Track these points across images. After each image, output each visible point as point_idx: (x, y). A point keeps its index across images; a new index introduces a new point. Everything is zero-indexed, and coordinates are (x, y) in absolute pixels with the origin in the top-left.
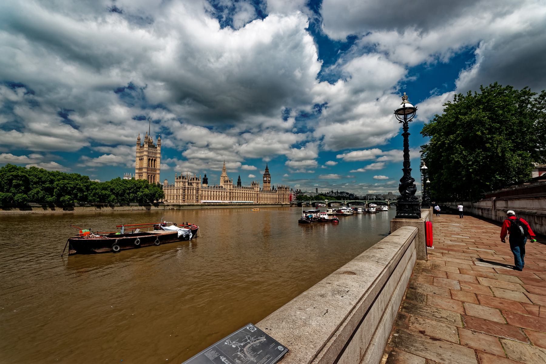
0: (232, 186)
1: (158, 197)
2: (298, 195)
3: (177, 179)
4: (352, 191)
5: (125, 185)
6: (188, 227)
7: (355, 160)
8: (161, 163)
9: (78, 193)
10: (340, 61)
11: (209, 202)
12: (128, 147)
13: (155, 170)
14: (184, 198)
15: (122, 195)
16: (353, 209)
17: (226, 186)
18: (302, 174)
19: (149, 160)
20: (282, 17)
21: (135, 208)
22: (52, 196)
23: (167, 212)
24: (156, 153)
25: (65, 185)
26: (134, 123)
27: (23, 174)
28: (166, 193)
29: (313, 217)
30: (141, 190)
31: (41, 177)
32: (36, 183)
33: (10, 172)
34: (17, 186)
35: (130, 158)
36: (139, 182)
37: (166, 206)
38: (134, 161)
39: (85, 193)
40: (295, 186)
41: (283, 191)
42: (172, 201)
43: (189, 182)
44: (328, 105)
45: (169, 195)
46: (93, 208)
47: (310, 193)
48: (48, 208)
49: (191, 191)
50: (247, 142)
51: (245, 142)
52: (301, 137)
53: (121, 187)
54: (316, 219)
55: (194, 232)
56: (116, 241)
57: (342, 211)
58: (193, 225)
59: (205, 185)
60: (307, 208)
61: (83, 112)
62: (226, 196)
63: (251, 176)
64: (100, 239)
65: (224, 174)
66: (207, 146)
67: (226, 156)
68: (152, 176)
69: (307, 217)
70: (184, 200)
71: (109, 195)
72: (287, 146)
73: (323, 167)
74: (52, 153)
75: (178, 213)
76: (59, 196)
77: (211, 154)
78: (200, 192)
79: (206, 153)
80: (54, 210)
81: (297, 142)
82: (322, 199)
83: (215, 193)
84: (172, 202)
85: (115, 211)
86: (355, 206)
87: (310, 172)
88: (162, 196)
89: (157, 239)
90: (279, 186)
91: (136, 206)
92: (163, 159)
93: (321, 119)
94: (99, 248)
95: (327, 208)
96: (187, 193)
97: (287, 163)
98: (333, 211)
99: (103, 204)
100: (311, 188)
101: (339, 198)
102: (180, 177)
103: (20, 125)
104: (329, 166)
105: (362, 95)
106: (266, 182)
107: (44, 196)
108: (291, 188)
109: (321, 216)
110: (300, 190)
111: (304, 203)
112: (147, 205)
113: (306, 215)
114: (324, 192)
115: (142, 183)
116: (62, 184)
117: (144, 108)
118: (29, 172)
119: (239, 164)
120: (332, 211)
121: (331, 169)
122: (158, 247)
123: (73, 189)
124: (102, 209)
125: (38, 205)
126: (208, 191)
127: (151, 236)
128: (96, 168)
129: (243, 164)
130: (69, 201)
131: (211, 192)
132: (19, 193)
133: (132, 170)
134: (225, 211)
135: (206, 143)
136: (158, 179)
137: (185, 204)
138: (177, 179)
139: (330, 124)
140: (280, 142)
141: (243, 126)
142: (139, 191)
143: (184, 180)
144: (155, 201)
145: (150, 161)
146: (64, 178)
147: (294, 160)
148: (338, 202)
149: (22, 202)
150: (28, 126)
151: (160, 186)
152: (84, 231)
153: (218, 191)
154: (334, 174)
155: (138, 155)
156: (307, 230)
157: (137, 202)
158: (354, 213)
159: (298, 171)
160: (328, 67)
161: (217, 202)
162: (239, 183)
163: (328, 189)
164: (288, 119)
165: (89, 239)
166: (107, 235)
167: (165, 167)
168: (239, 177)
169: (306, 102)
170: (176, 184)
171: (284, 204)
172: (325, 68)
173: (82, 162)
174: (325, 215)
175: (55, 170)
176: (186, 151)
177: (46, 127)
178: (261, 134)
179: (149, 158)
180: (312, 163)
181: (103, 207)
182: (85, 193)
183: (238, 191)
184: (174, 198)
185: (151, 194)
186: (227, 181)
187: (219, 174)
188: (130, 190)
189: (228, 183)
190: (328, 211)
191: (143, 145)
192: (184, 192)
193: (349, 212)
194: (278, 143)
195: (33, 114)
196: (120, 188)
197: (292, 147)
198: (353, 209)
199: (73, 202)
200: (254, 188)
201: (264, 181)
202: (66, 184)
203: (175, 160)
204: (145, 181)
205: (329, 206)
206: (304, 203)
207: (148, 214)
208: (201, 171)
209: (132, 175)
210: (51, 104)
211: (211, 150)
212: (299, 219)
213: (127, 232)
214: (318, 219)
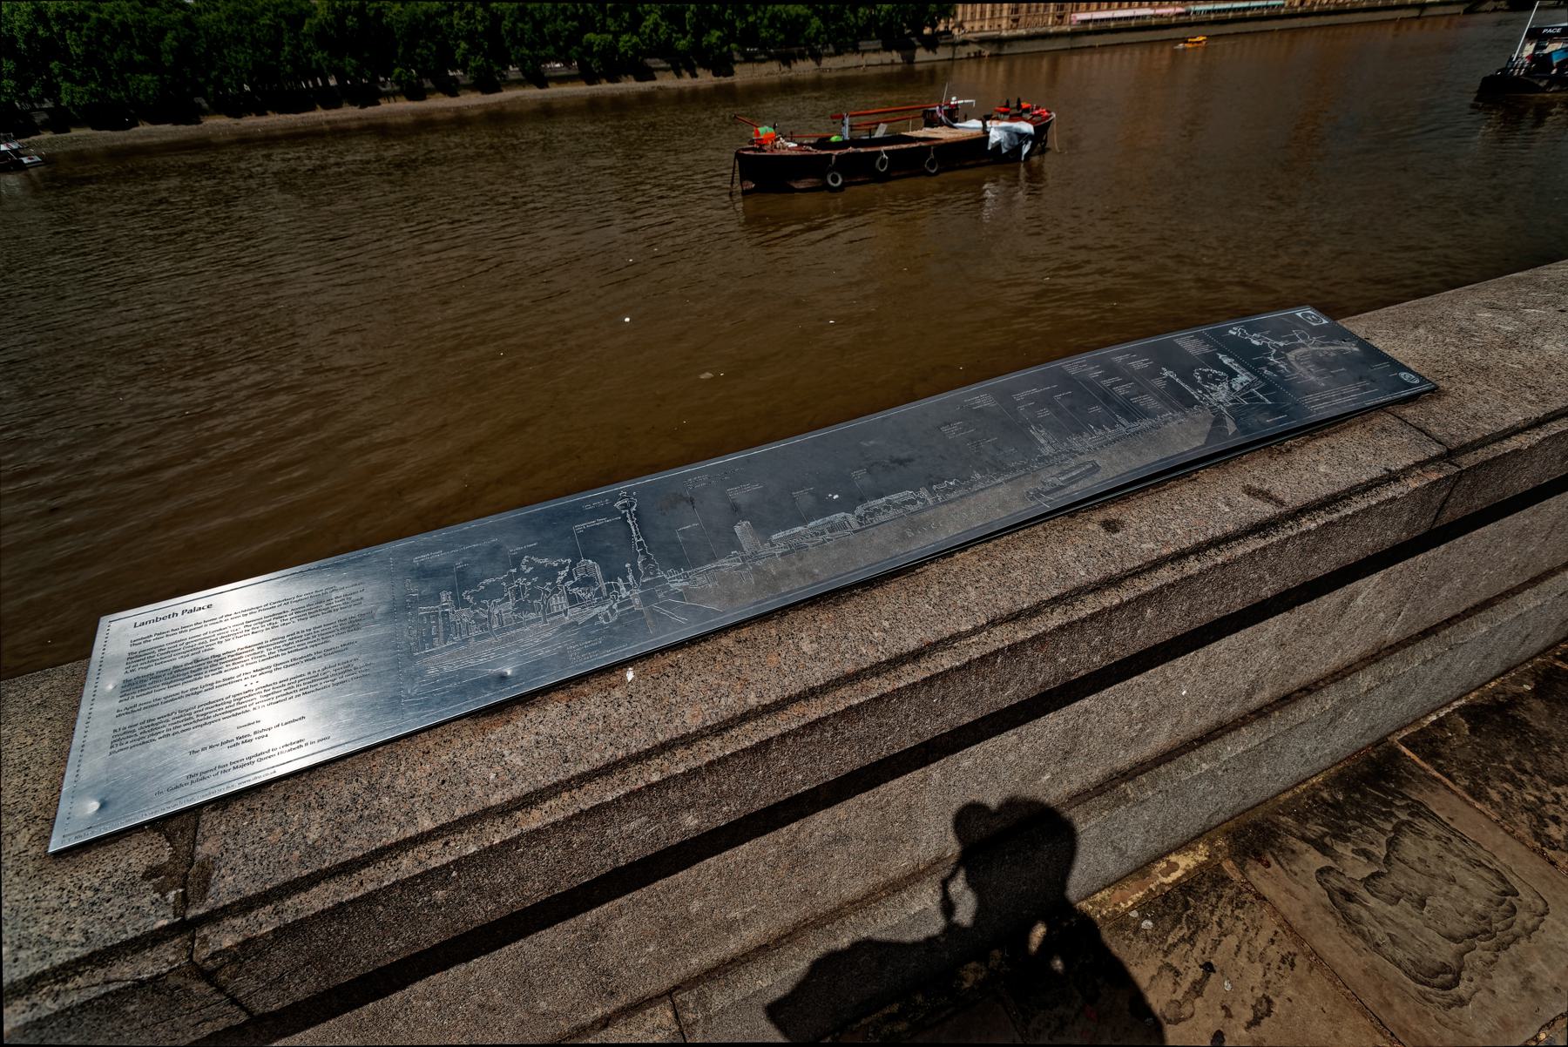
11: (1102, 20)
21: (874, 58)
22: (685, 34)
37: (957, 44)
39: (751, 19)
42: (977, 25)
46: (774, 66)
48: (683, 71)
56: (834, 158)
58: (1038, 108)
64: (799, 153)
71: (807, 19)
75: (993, 65)
80: (696, 76)
84: (976, 29)
85: (824, 70)
91: (875, 51)
94: (798, 179)
99: (795, 50)
107: (670, 36)
112: (906, 48)
113: (1536, 48)
124: (794, 66)
125: (663, 65)
127: (914, 145)
130: (720, 48)
144: (927, 31)
152: (762, 130)
157: (878, 38)
161: (1132, 18)
165: (777, 153)
166: (812, 142)
181: (796, 62)
182: (751, 19)
199: (730, 50)
207: (908, 77)
212: (1492, 69)
213: (857, 134)
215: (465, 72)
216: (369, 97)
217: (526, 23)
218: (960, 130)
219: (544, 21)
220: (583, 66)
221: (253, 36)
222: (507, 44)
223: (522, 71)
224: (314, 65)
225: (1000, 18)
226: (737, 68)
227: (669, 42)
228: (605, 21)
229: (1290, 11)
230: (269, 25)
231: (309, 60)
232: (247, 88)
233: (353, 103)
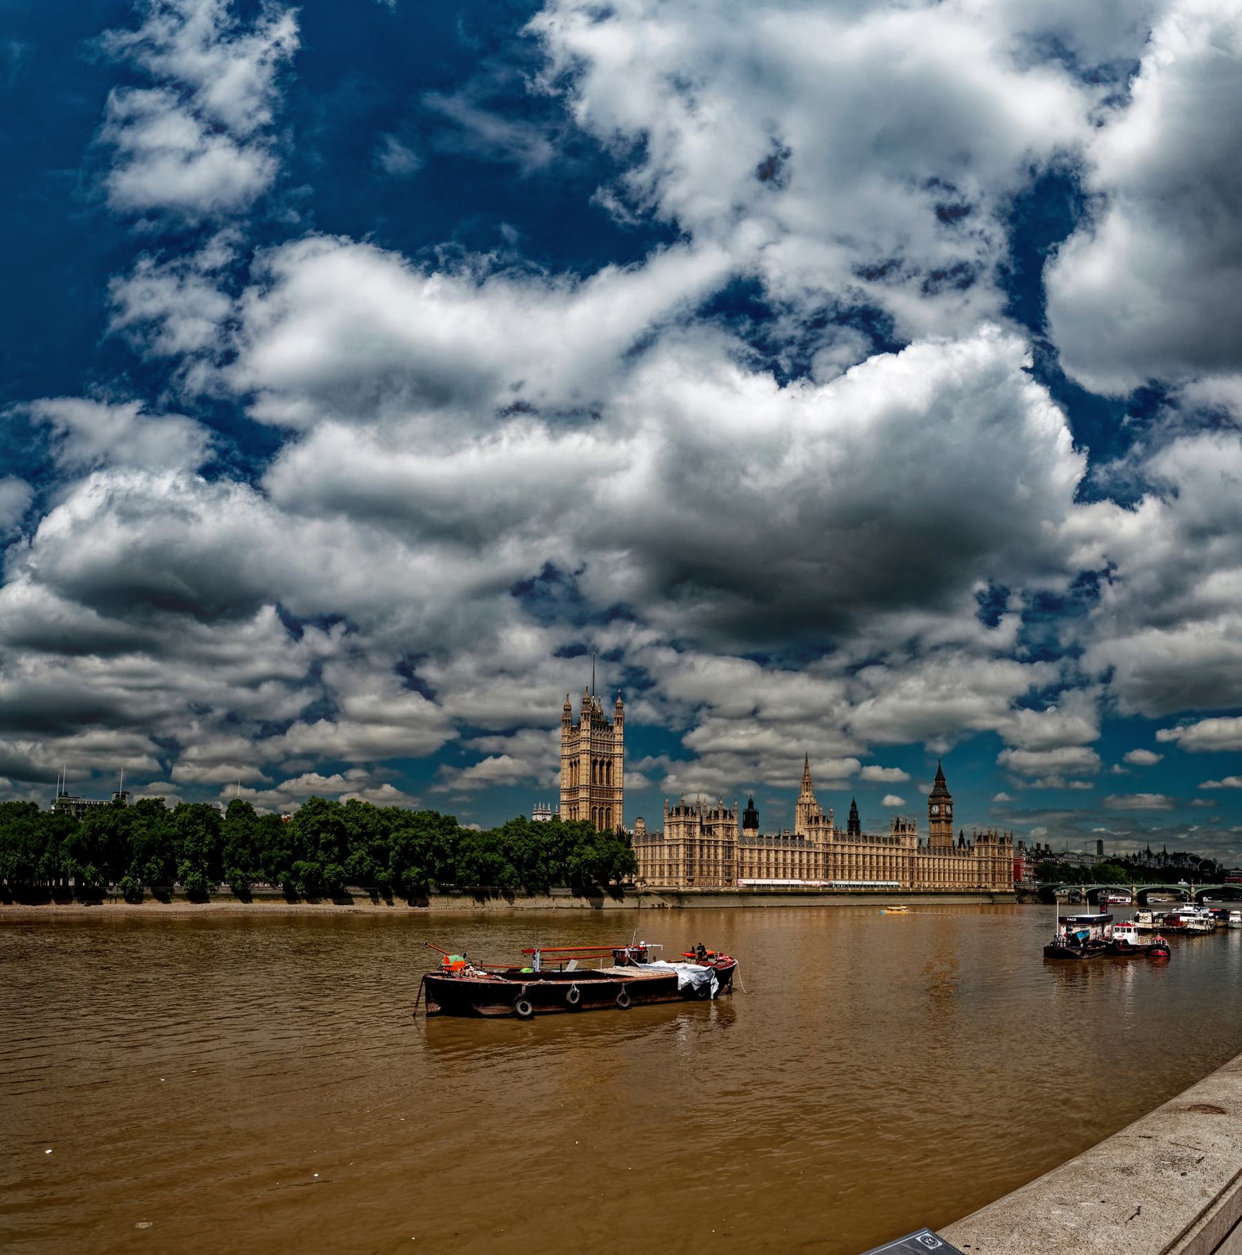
0: (831, 835)
1: (619, 870)
2: (1042, 861)
3: (670, 815)
4: (1208, 851)
5: (537, 837)
6: (706, 960)
7: (1214, 747)
8: (625, 770)
9: (434, 861)
10: (1137, 448)
11: (764, 885)
12: (542, 732)
13: (610, 791)
14: (691, 873)
15: (531, 864)
16: (1216, 913)
17: (813, 834)
18: (1050, 792)
19: (594, 763)
20: (943, 344)
22: (387, 868)
23: (647, 916)
24: (611, 745)
25: (408, 839)
26: (557, 667)
27: (337, 818)
28: (642, 858)
29: (1092, 937)
30: (575, 849)
31: (367, 824)
32: (358, 838)
33: (316, 814)
34: (327, 846)
35: (547, 761)
36: (571, 828)
37: (641, 895)
38: (557, 770)
39: (450, 861)
40: (1032, 832)
41: (994, 847)
42: (657, 882)
43: (704, 823)
44: (1119, 572)
45: (649, 863)
47: (1078, 856)
48: (381, 899)
49: (709, 851)
50: (874, 693)
51: (869, 693)
52: (1046, 673)
53: (527, 842)
54: (1101, 943)
55: (725, 976)
57: (1183, 919)
58: (721, 955)
59: (749, 833)
60: (1071, 908)
61: (444, 654)
62: (813, 867)
63: (891, 800)
65: (807, 797)
66: (754, 715)
67: (809, 740)
68: (602, 808)
69: (1073, 939)
70: (692, 877)
71: (502, 866)
72: (1002, 702)
73: (1117, 768)
74: (384, 764)
75: (676, 918)
76: (400, 867)
77: (767, 738)
78: (736, 852)
79: (752, 735)
81: (1032, 688)
82: (1113, 878)
83: (781, 855)
84: (657, 884)
85: (516, 908)
86: (1220, 904)
87: (1078, 785)
88: (630, 866)
89: (623, 991)
90: (978, 834)
91: (565, 897)
92: (632, 756)
93: (1098, 618)
94: (487, 1004)
95: (1134, 908)
96: (698, 857)
97: (1004, 756)
98: (1153, 918)
99: (489, 888)
100: (1083, 840)
101: (1170, 875)
102: (678, 810)
103: (331, 706)
104: (1138, 768)
105: (1217, 545)
106: (939, 821)
107: (373, 868)
108: (1017, 837)
109: (1116, 936)
110: (1047, 846)
111: (1063, 891)
113: (1067, 930)
114: (1122, 853)
115: (578, 831)
116: (404, 838)
117: (579, 622)
118: (346, 812)
119: (852, 764)
120: (1149, 920)
121: (1141, 779)
122: (626, 1014)
123: (426, 848)
124: (487, 903)
125: (363, 893)
126: (760, 850)
127: (605, 981)
128: (471, 793)
129: (865, 762)
130: (418, 882)
131: (768, 855)
132: (331, 863)
133: (552, 795)
134: (815, 913)
135: (749, 704)
136: (617, 817)
137: (694, 889)
138: (670, 815)
139: (1129, 634)
140: (978, 689)
141: (861, 647)
142: (569, 854)
143: (690, 819)
144: (612, 882)
145: (598, 767)
146: (407, 825)
147: (1026, 746)
148: (1170, 891)
149: (336, 884)
150: (344, 707)
151: (625, 839)
153: (789, 848)
154: (1155, 793)
155: (567, 752)
156: (1071, 976)
158: (1216, 927)
159: (1039, 784)
160: (1104, 462)
161: (788, 885)
162: (854, 825)
163: (1135, 844)
164: (1000, 617)
165: (465, 980)
167: (636, 781)
168: (854, 805)
169: (1050, 565)
170: (667, 829)
171: (997, 890)
172: (1097, 466)
173: (441, 780)
174: (1129, 931)
175: (390, 805)
176: (693, 730)
177: (373, 703)
178: (917, 667)
179: (593, 758)
180: (1083, 756)
182: (450, 861)
183: (852, 850)
184: (662, 873)
185: (601, 860)
186: (817, 819)
187: (791, 796)
188: (548, 850)
189: (821, 826)
190: (1137, 919)
191: (579, 724)
192: (691, 855)
193: (1201, 922)
194: (970, 693)
195: (353, 677)
196: (526, 845)
197: (1016, 705)
198: (1216, 913)
199: (426, 883)
200: (902, 840)
201: (931, 816)
202: (411, 839)
203: (664, 759)
204: (585, 823)
205: (1141, 902)
206: (1063, 891)
207: (599, 920)
208: (737, 788)
209: (553, 807)
210: (382, 647)
211: (765, 723)
212: (1048, 944)
214: (1106, 944)
215: (182, 884)
216: (95, 896)
217: (245, 849)
218: (651, 970)
219: (262, 848)
220: (288, 887)
221: (25, 844)
222: (225, 865)
223: (233, 888)
224: (62, 870)
225: (677, 877)
226: (432, 901)
227: (371, 873)
228: (316, 852)
229: (905, 890)
230: (40, 838)
231: (60, 866)
232: (5, 882)
233: (81, 901)
